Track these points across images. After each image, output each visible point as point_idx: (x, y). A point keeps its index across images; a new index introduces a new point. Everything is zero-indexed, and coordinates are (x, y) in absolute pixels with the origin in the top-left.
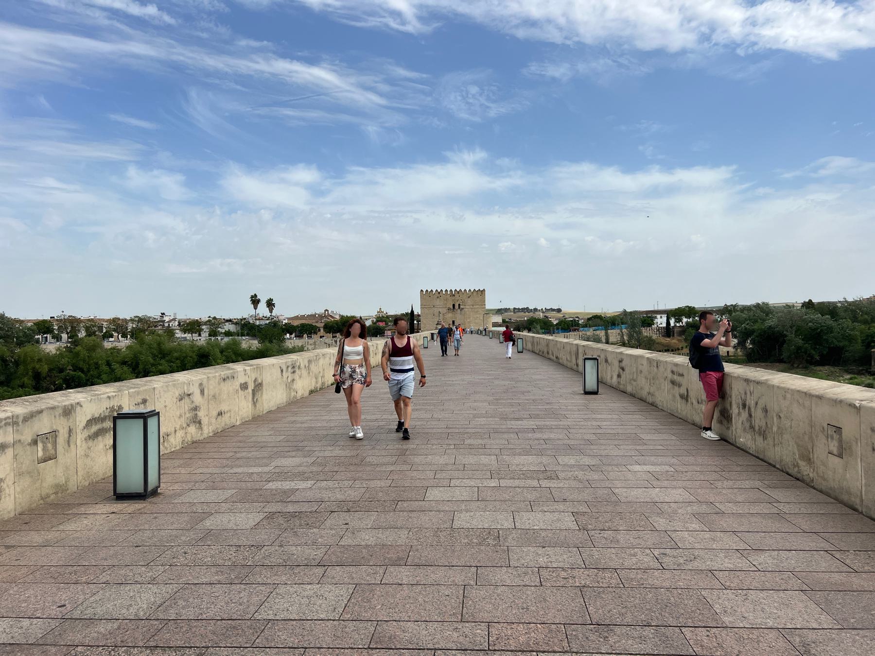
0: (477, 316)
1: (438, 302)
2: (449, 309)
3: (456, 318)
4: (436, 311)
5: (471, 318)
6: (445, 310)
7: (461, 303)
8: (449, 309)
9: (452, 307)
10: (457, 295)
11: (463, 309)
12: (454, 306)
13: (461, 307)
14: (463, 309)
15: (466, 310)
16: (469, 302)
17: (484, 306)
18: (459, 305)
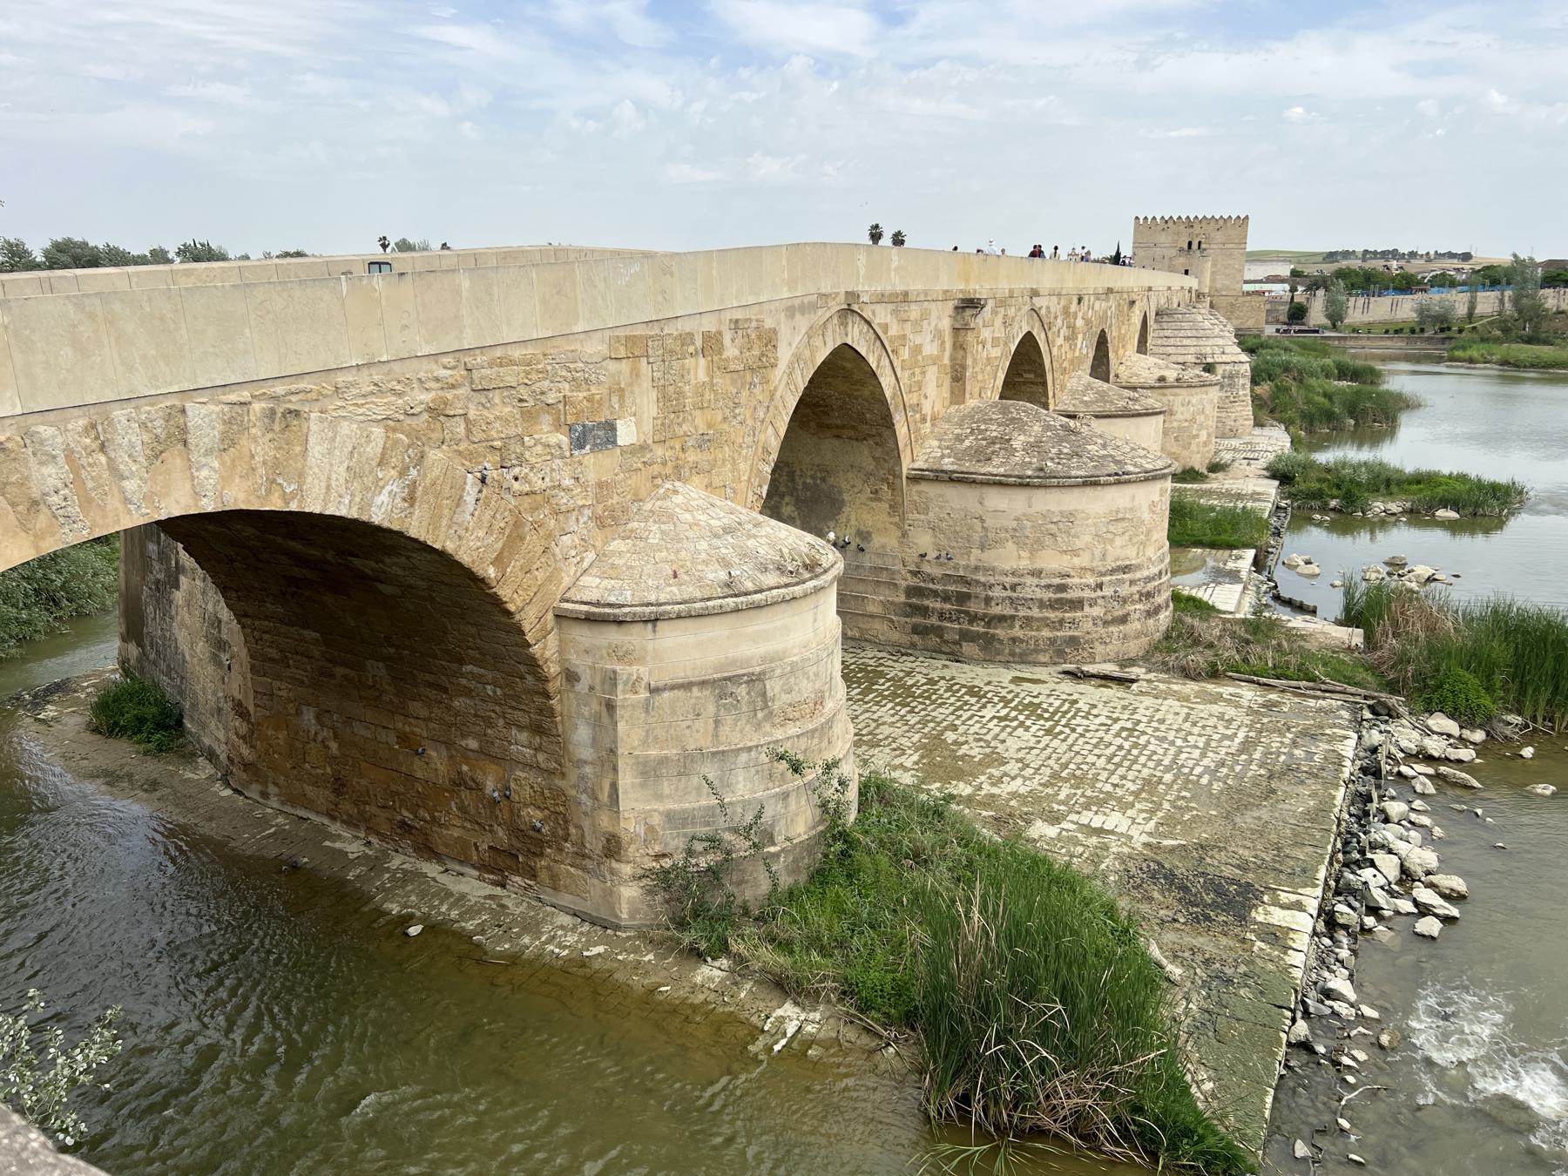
1: (1163, 239)
2: (1181, 250)
6: (1174, 252)
8: (1181, 250)
9: (1186, 246)
12: (1190, 244)
13: (1203, 246)
16: (1219, 237)
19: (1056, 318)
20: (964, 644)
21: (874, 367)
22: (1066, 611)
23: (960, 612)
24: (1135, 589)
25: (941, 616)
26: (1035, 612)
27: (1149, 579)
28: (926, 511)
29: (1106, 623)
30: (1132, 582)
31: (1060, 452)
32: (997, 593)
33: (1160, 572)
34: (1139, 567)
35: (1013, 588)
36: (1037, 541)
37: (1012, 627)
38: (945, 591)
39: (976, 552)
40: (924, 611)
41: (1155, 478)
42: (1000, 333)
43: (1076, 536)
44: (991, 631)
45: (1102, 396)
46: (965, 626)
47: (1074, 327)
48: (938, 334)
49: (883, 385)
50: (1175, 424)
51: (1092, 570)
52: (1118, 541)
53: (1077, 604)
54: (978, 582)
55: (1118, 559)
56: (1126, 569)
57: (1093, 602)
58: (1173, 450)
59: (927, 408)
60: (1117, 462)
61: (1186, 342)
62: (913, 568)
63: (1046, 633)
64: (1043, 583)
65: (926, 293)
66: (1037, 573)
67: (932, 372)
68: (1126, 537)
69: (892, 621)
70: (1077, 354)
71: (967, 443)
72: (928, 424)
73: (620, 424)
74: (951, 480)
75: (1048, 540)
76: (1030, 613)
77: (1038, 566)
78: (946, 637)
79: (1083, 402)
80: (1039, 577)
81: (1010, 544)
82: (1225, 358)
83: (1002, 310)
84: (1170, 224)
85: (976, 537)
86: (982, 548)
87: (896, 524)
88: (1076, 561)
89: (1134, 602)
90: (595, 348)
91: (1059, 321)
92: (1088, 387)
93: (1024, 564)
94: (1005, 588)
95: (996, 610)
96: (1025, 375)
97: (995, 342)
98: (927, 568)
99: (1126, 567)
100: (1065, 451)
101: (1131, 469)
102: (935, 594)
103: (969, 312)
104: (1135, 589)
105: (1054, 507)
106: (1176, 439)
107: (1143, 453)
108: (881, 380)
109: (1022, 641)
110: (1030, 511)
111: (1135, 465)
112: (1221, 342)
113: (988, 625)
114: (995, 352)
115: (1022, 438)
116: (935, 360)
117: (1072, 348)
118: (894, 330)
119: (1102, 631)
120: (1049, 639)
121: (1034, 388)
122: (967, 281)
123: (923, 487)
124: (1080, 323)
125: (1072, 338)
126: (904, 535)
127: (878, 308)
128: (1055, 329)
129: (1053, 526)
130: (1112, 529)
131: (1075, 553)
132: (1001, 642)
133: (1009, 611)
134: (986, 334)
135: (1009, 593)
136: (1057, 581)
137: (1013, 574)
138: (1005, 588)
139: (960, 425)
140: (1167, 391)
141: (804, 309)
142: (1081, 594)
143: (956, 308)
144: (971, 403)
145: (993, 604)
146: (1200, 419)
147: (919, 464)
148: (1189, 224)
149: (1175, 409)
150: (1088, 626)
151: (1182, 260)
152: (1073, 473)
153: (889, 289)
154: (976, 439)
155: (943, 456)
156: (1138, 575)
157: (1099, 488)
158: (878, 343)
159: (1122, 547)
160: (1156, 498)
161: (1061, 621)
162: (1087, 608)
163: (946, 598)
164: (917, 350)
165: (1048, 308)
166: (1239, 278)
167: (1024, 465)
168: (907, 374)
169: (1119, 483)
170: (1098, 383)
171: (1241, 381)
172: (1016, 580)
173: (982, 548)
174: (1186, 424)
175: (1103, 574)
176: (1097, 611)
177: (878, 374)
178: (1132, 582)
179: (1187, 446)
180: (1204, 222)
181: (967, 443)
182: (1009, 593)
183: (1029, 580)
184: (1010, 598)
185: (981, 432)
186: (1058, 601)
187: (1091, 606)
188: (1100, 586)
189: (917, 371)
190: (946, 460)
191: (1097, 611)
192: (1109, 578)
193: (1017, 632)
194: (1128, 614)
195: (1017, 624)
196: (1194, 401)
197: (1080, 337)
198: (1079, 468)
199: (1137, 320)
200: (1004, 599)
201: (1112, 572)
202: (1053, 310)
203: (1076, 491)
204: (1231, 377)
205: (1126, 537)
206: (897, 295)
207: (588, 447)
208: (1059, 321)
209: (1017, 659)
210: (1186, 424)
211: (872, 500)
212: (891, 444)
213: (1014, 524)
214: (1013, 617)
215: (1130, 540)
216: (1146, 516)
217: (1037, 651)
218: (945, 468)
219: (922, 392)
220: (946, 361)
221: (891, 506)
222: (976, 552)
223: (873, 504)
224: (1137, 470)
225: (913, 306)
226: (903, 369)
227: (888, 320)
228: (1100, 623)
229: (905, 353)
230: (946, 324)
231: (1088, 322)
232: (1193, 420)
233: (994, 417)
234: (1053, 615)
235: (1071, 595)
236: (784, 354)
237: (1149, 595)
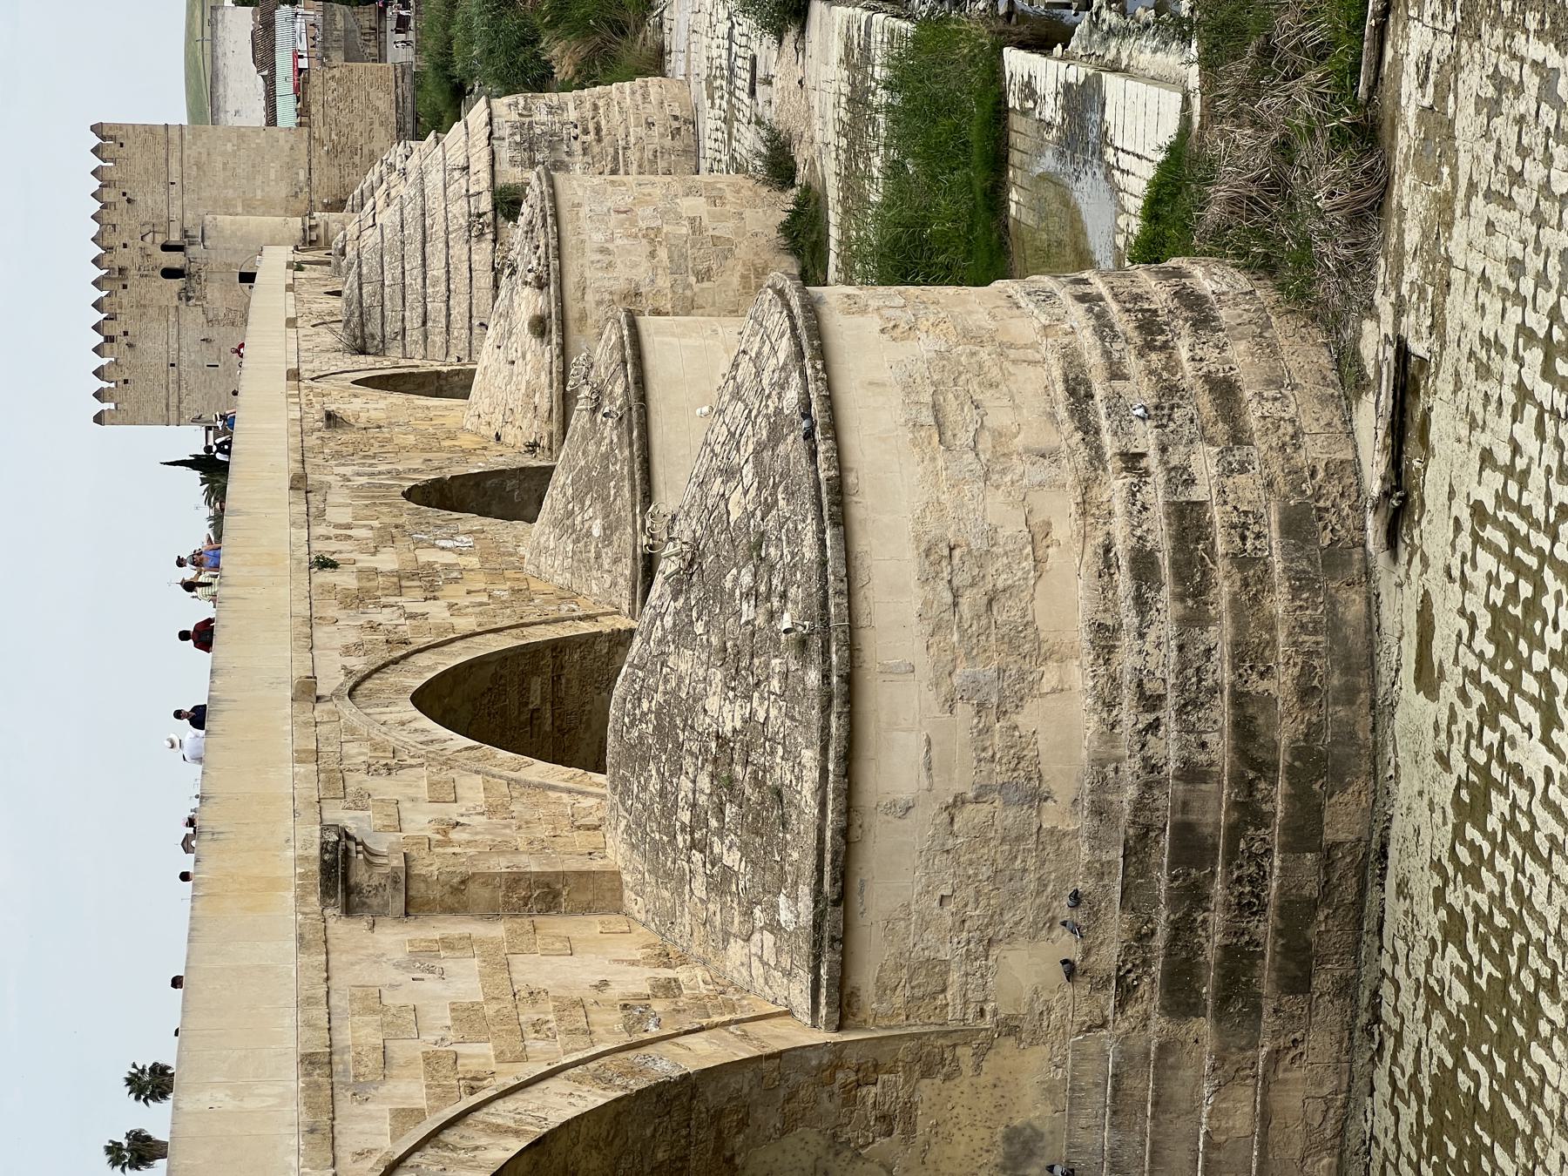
0: (219, 166)
1: (154, 348)
2: (185, 295)
3: (230, 265)
4: (192, 355)
5: (230, 193)
6: (193, 316)
7: (160, 239)
8: (185, 295)
9: (176, 284)
10: (121, 258)
11: (185, 233)
12: (169, 273)
13: (175, 238)
14: (185, 233)
15: (189, 215)
16: (150, 200)
17: (174, 135)
18: (166, 248)
19: (374, 627)
20: (1329, 835)
21: (517, 1145)
22: (1211, 551)
23: (1232, 853)
24: (1133, 365)
25: (1248, 906)
26: (1220, 635)
27: (1103, 327)
28: (937, 968)
29: (1238, 437)
30: (1116, 373)
31: (752, 593)
32: (1168, 748)
33: (1082, 298)
34: (1070, 357)
35: (1151, 702)
36: (1011, 642)
37: (1268, 701)
38: (1174, 900)
39: (1052, 816)
40: (1238, 959)
41: (817, 331)
42: (417, 782)
43: (991, 535)
44: (1283, 759)
45: (590, 485)
46: (1275, 835)
47: (399, 575)
48: (423, 960)
49: (570, 1113)
50: (664, 282)
51: (1087, 485)
54: (1139, 806)
55: (1052, 415)
56: (1078, 392)
57: (1181, 477)
58: (736, 281)
59: (637, 981)
60: (775, 436)
61: (436, 269)
62: (1109, 999)
63: (1279, 603)
64: (1130, 619)
65: (306, 1002)
66: (1104, 638)
67: (532, 970)
69: (1275, 1056)
70: (474, 562)
71: (732, 859)
72: (681, 974)
74: (842, 898)
75: (1006, 613)
76: (1223, 652)
77: (1081, 637)
78: (1311, 889)
79: (607, 539)
80: (1116, 630)
81: (1027, 718)
82: (480, 164)
83: (353, 780)
84: (115, 329)
85: (1009, 817)
86: (1037, 798)
87: (980, 1055)
88: (1065, 529)
89: (1172, 366)
91: (384, 617)
92: (564, 525)
93: (1079, 675)
94: (1154, 726)
95: (1220, 748)
96: (535, 701)
97: (444, 793)
98: (1108, 956)
99: (1072, 392)
100: (746, 579)
101: (792, 396)
102: (1182, 929)
103: (360, 875)
104: (1133, 365)
105: (912, 601)
106: (704, 276)
107: (746, 367)
108: (555, 1120)
109: (1307, 671)
110: (923, 663)
111: (783, 386)
112: (435, 179)
113: (1265, 768)
114: (472, 790)
115: (712, 704)
116: (498, 963)
117: (455, 575)
118: (411, 1090)
119: (1260, 447)
120: (1295, 592)
121: (571, 673)
122: (273, 884)
123: (866, 978)
124: (387, 561)
125: (429, 581)
126: (1009, 1028)
127: (348, 1142)
128: (406, 628)
129: (964, 602)
130: (965, 438)
131: (1039, 536)
132: (1313, 731)
133: (1222, 711)
134: (420, 822)
135: (1168, 714)
136: (1124, 581)
137: (1110, 706)
138: (1154, 726)
139: (681, 881)
140: (573, 313)
142: (1158, 510)
143: (348, 911)
144: (616, 853)
145: (1202, 758)
146: (646, 217)
147: (798, 993)
148: (113, 277)
149: (621, 286)
150: (1248, 487)
152: (809, 553)
153: (292, 1113)
154: (720, 833)
155: (774, 927)
156: (1093, 359)
157: (851, 479)
158: (450, 1136)
159: (1016, 407)
161: (1241, 561)
162: (1198, 493)
163: (1192, 896)
164: (467, 1018)
165: (347, 651)
166: (261, 139)
167: (791, 693)
168: (536, 1045)
169: (834, 428)
170: (555, 498)
171: (541, 116)
172: (1128, 697)
173: (1037, 798)
174: (663, 253)
175: (1097, 455)
176: (1204, 462)
177: (537, 1131)
178: (1116, 373)
179: (723, 248)
180: (111, 239)
181: (732, 859)
182: (1168, 714)
183: (1127, 658)
184: (1181, 710)
185: (698, 821)
186: (1180, 576)
187: (1190, 482)
188: (1132, 461)
189: (528, 1014)
190: (785, 916)
191: (1204, 462)
192: (1107, 438)
193: (1281, 684)
194: (1208, 378)
195: (1258, 685)
196: (598, 237)
197: (425, 556)
198: (795, 538)
199: (379, 405)
200: (1187, 728)
201: (1088, 429)
202: (352, 637)
203: (865, 543)
204: (529, 144)
206: (313, 1087)
208: (384, 617)
209: (1362, 682)
210: (663, 253)
211: (910, 1131)
212: (743, 1082)
213: (964, 711)
214: (1240, 699)
216: (924, 346)
217: (1334, 626)
218: (806, 918)
219: (590, 996)
220: (498, 930)
221: (927, 1073)
222: (1052, 816)
223: (923, 1125)
224: (795, 379)
225: (344, 1037)
226: (522, 1058)
228: (1239, 454)
229: (479, 1054)
230: (394, 938)
231: (387, 537)
232: (652, 237)
233: (655, 784)
234: (1224, 588)
235: (1160, 537)
237: (1149, 325)
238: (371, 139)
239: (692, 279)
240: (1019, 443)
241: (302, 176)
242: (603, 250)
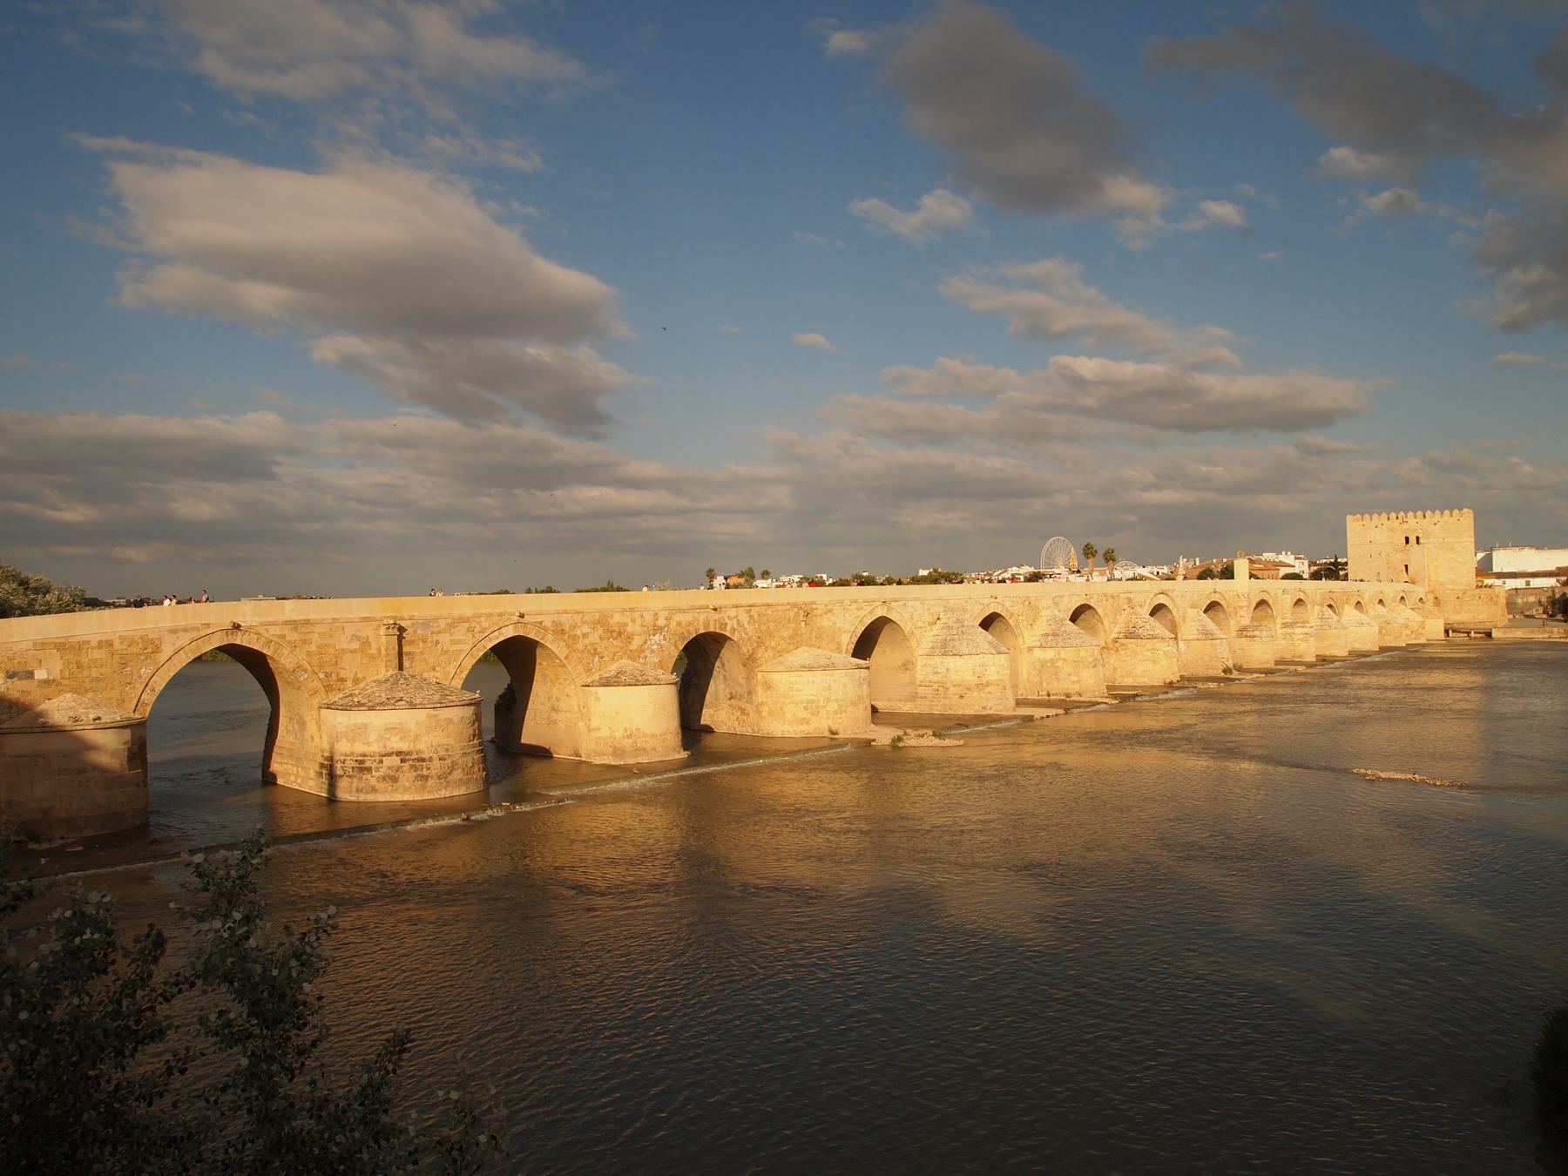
7: (1420, 536)
12: (1407, 540)
13: (1421, 541)
15: (1431, 546)
18: (1418, 538)
52: (393, 739)
53: (369, 770)
56: (399, 753)
58: (805, 716)
64: (354, 759)
66: (352, 754)
68: (398, 737)
73: (36, 672)
90: (24, 646)
131: (369, 744)
141: (185, 630)
151: (1399, 556)
160: (423, 718)
176: (378, 774)
205: (398, 737)
207: (16, 679)
213: (344, 730)
215: (401, 738)
216: (412, 726)
227: (286, 632)
236: (167, 650)
238: (1466, 612)
239: (805, 705)
240: (387, 742)
241: (1450, 587)
242: (813, 682)
